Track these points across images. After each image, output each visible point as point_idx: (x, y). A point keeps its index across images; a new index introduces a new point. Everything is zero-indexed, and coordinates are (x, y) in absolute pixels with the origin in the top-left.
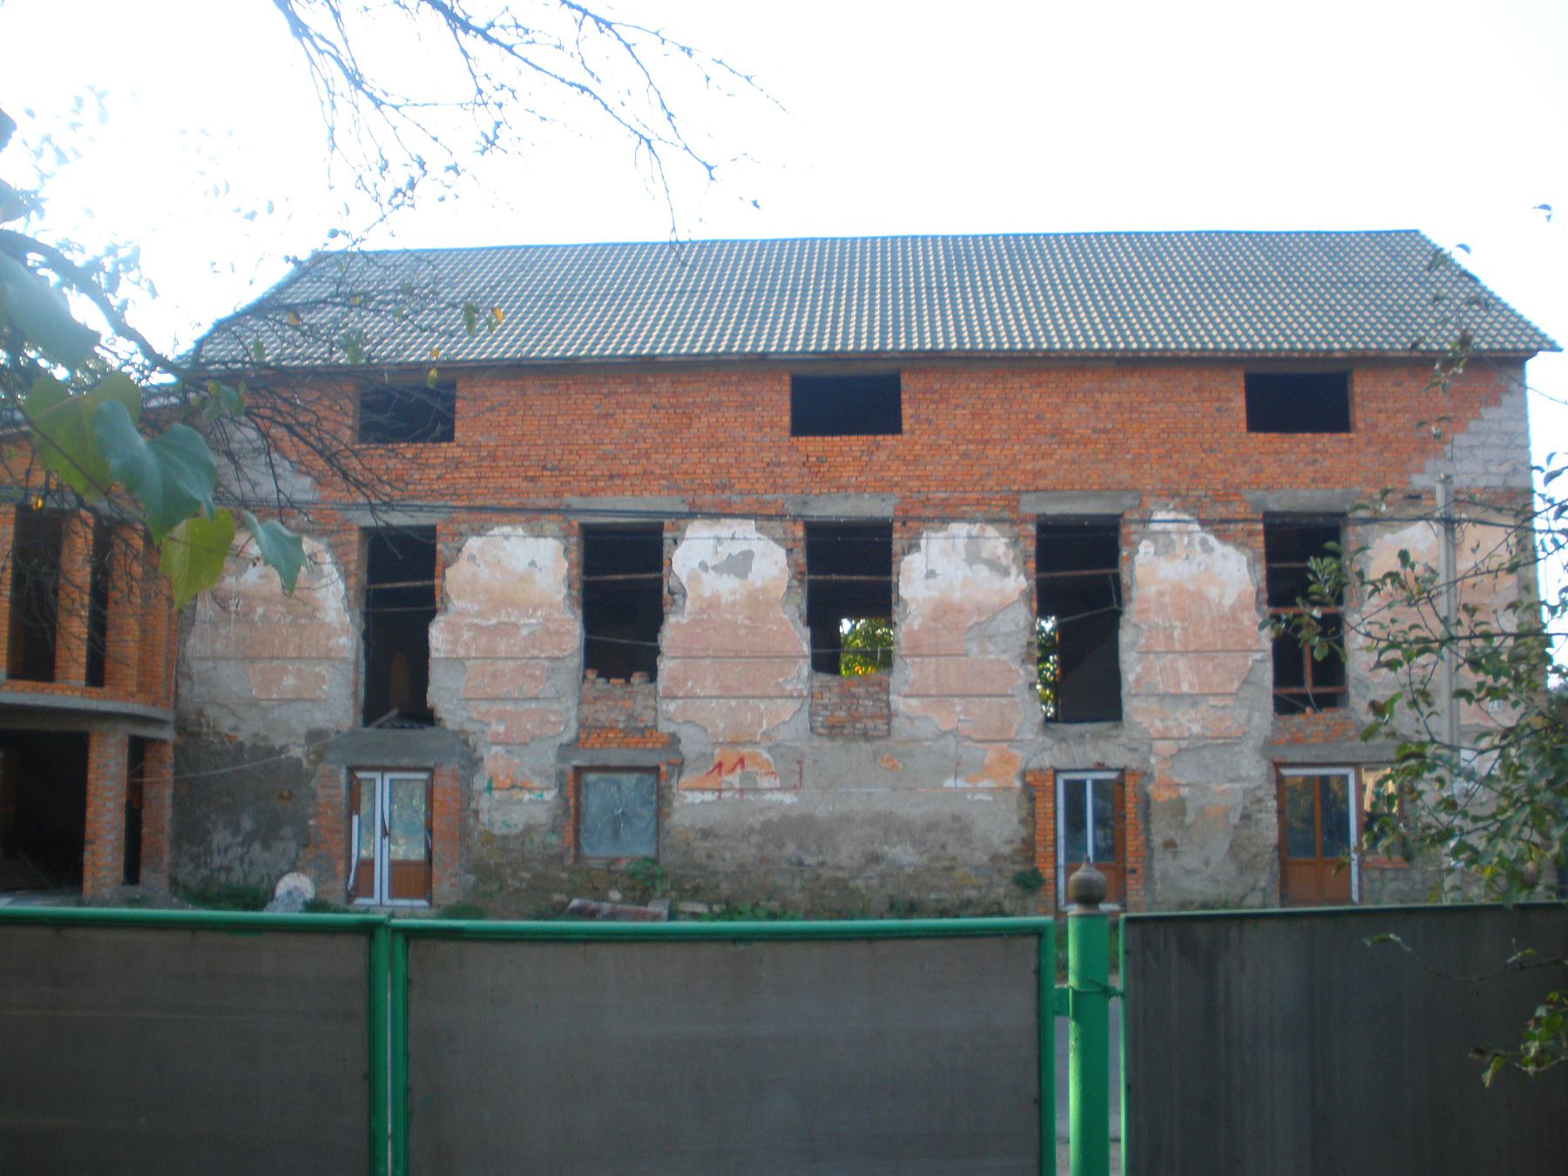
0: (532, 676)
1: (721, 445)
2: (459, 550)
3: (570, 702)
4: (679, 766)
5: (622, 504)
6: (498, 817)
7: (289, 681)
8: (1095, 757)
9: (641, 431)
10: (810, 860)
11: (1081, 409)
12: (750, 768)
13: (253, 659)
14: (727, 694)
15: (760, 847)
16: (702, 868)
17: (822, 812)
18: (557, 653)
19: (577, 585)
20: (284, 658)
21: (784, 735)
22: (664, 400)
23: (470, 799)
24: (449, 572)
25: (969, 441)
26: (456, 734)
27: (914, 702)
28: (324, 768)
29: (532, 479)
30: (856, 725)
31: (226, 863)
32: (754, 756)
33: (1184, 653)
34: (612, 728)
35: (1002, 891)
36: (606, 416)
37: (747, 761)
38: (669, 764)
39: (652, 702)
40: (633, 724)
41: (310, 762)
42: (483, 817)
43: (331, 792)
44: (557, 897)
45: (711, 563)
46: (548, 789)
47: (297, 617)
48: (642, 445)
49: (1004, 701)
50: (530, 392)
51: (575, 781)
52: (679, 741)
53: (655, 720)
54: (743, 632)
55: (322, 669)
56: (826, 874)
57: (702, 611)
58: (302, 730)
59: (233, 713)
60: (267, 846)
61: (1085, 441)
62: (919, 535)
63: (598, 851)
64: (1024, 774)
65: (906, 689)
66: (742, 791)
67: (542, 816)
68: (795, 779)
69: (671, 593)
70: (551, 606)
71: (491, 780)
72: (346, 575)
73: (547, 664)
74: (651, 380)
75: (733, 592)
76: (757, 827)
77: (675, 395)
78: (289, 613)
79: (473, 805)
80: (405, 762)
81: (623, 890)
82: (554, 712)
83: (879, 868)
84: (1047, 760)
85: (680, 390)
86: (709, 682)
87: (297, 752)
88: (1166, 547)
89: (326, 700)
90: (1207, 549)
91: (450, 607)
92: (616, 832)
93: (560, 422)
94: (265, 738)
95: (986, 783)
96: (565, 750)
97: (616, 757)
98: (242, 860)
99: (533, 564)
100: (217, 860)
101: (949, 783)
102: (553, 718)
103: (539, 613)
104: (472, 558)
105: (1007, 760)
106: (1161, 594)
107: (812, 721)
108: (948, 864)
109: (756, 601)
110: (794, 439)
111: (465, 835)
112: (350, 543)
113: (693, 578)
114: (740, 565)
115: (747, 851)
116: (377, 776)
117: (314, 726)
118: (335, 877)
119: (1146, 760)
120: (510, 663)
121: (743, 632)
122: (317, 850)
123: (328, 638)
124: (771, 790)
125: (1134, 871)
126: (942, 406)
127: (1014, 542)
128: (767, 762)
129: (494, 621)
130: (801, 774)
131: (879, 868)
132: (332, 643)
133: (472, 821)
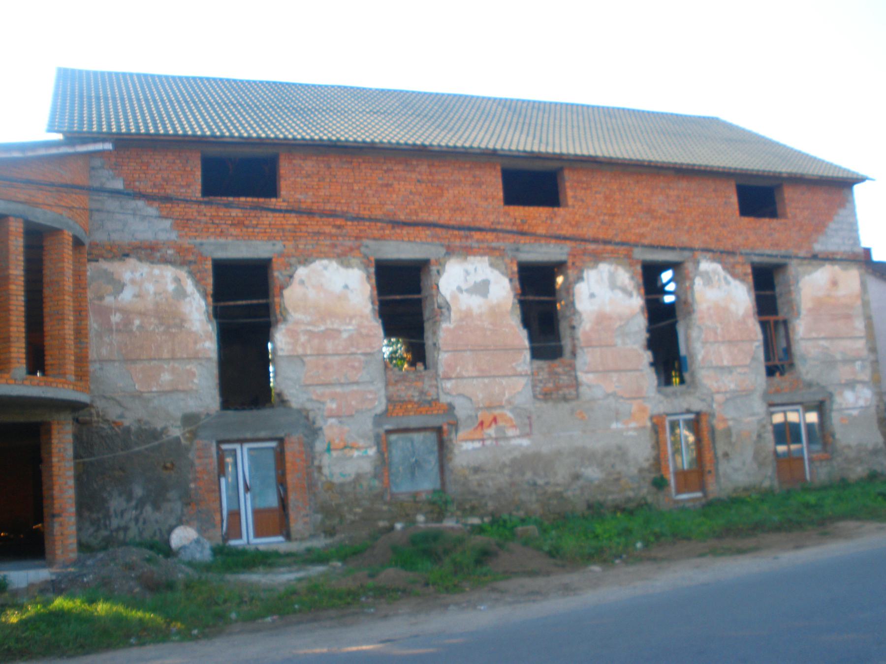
0: (353, 367)
1: (463, 209)
2: (291, 277)
3: (380, 385)
4: (455, 425)
5: (401, 249)
6: (337, 470)
7: (166, 377)
8: (685, 406)
9: (411, 197)
10: (541, 482)
11: (663, 198)
12: (501, 424)
13: (134, 361)
14: (483, 374)
15: (511, 476)
16: (475, 493)
17: (545, 449)
18: (369, 350)
19: (377, 303)
20: (160, 359)
21: (520, 400)
22: (425, 177)
23: (313, 458)
24: (287, 293)
25: (605, 214)
26: (299, 411)
27: (591, 376)
28: (198, 443)
29: (339, 227)
30: (558, 392)
31: (123, 523)
32: (502, 416)
33: (723, 342)
34: (410, 402)
35: (645, 490)
36: (387, 185)
37: (499, 419)
38: (449, 424)
39: (434, 382)
40: (423, 397)
41: (186, 439)
42: (326, 471)
43: (207, 461)
44: (381, 524)
45: (464, 287)
46: (370, 447)
47: (169, 327)
48: (412, 207)
49: (638, 374)
50: (333, 165)
51: (382, 442)
52: (454, 408)
53: (438, 394)
54: (488, 333)
55: (192, 367)
56: (550, 490)
57: (462, 319)
58: (179, 414)
59: (119, 404)
60: (156, 507)
61: (664, 218)
62: (581, 271)
63: (403, 488)
64: (651, 418)
65: (586, 368)
66: (497, 439)
67: (367, 467)
68: (527, 430)
69: (440, 307)
70: (362, 317)
71: (329, 444)
72: (205, 295)
73: (362, 358)
74: (414, 163)
75: (480, 307)
76: (508, 462)
77: (431, 174)
78: (162, 324)
79: (316, 463)
80: (262, 434)
81: (426, 514)
82: (370, 392)
83: (581, 482)
84: (661, 409)
85: (434, 170)
86: (470, 367)
87: (176, 432)
88: (708, 279)
89: (197, 391)
90: (728, 283)
91: (289, 318)
92: (413, 474)
93: (356, 188)
94: (147, 423)
95: (633, 425)
96: (379, 419)
97: (414, 421)
98: (137, 520)
99: (346, 287)
100: (115, 522)
101: (614, 426)
102: (370, 396)
103: (354, 322)
104: (302, 282)
105: (643, 410)
106: (709, 308)
107: (534, 391)
108: (615, 476)
109: (494, 312)
110: (507, 208)
111: (311, 486)
112: (206, 271)
113: (454, 297)
114: (482, 288)
115: (502, 480)
116: (237, 446)
117: (189, 411)
118: (214, 527)
119: (710, 406)
120: (337, 358)
121: (488, 333)
122: (197, 507)
123: (196, 343)
124: (514, 437)
125: (710, 472)
126: (589, 192)
127: (632, 278)
128: (511, 420)
129: (322, 328)
130: (530, 425)
131: (581, 482)
132: (199, 346)
133: (316, 475)
